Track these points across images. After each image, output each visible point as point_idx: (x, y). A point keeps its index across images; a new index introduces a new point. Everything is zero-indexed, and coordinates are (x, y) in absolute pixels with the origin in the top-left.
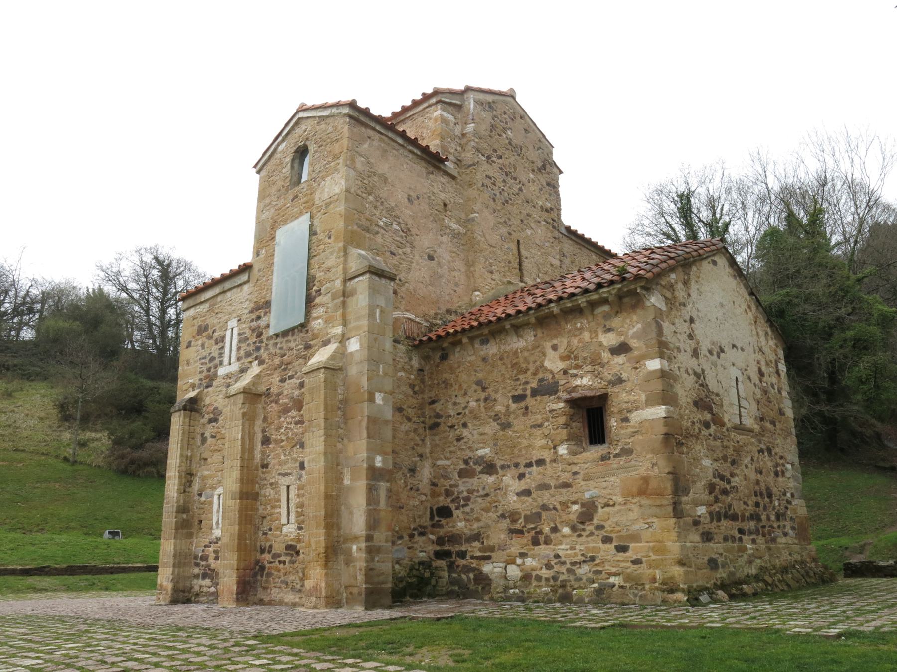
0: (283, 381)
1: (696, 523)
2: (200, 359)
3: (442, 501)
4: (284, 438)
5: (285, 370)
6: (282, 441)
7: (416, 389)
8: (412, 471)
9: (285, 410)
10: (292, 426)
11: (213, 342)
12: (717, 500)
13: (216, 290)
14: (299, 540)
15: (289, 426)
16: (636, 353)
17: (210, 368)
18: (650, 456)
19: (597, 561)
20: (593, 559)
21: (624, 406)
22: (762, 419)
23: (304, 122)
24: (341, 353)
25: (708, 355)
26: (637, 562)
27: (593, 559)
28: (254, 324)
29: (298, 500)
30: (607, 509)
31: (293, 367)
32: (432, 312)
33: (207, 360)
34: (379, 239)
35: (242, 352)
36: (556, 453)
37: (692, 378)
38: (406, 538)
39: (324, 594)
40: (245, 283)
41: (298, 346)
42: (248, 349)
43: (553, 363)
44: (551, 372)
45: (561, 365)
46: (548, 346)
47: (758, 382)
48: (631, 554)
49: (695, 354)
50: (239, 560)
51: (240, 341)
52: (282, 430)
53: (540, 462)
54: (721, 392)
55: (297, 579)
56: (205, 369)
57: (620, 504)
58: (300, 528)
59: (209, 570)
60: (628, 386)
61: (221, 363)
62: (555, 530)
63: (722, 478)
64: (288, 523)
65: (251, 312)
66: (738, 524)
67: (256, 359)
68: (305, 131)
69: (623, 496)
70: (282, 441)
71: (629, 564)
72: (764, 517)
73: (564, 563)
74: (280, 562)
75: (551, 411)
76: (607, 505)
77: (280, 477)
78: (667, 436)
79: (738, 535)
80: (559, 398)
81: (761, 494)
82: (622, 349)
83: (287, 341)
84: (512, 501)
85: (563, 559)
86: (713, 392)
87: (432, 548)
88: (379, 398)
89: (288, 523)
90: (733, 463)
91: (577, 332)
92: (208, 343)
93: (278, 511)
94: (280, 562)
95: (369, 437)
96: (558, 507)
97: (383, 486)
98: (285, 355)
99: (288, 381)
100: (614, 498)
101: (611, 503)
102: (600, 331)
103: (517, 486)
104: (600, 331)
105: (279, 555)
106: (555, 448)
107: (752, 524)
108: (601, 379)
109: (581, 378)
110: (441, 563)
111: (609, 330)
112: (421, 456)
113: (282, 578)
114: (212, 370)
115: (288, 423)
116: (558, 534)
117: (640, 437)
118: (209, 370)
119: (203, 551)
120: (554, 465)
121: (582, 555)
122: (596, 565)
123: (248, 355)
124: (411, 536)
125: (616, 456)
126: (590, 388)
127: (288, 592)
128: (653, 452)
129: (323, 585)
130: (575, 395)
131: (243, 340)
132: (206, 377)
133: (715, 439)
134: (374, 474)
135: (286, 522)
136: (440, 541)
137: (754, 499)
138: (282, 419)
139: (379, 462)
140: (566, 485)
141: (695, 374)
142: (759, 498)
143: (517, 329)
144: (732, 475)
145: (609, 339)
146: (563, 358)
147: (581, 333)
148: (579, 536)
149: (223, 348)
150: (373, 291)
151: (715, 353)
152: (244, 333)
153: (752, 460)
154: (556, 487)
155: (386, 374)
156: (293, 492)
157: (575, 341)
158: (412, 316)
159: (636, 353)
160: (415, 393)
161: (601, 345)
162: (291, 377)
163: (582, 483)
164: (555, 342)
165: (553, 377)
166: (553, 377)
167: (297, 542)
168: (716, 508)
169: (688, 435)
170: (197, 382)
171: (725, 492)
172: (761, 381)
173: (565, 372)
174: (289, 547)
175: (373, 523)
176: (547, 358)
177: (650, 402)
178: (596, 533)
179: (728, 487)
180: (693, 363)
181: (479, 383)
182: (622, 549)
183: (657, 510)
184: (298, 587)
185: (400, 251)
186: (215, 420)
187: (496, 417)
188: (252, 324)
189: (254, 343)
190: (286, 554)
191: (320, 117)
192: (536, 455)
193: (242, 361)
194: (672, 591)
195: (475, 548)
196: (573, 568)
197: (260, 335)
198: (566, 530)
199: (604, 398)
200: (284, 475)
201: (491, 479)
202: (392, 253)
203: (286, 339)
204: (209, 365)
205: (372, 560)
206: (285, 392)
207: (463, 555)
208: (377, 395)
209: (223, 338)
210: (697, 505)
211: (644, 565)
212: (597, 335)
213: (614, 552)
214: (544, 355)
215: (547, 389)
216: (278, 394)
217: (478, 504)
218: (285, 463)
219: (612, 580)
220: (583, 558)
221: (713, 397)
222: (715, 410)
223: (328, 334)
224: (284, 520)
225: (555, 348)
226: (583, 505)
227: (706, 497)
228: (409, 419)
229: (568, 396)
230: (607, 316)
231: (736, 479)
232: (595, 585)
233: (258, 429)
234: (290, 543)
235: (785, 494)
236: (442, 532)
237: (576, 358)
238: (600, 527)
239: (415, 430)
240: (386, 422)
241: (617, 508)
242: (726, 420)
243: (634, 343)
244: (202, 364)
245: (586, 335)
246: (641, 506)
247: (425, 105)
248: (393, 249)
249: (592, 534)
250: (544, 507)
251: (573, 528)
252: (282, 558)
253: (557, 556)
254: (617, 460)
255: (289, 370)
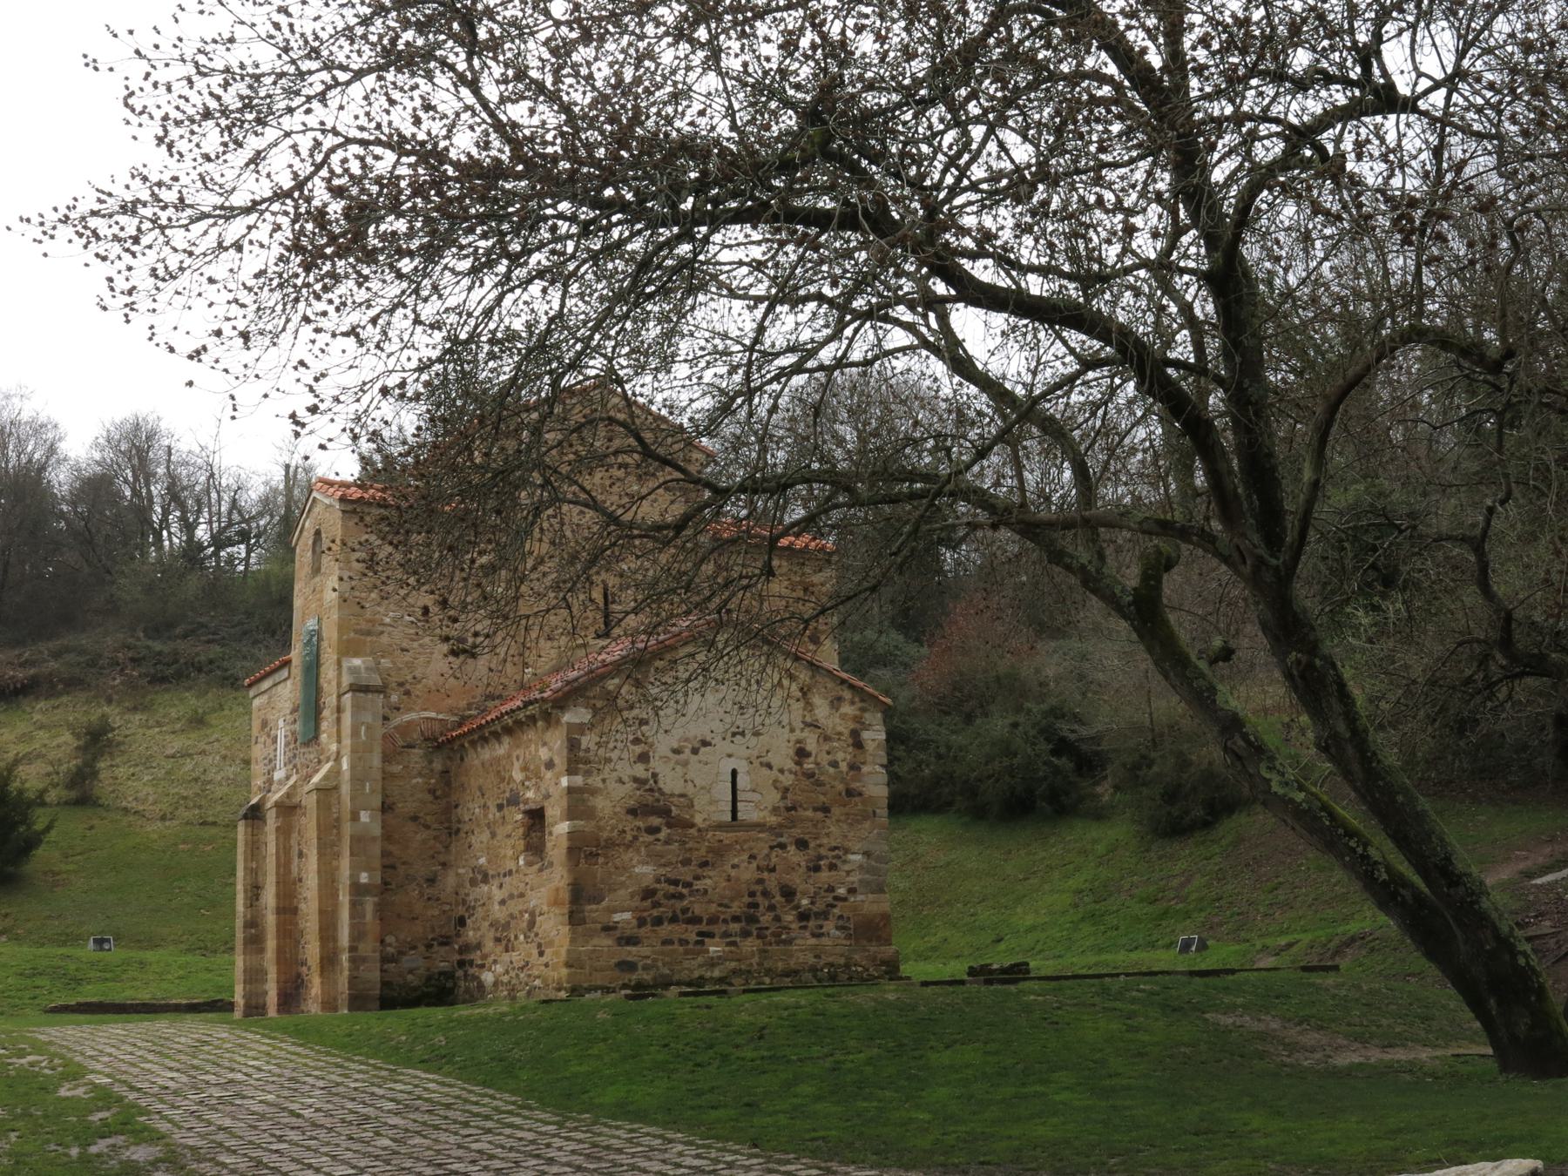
1: (608, 929)
3: (461, 911)
7: (439, 793)
8: (431, 881)
12: (656, 905)
22: (788, 809)
24: (336, 772)
25: (671, 755)
32: (463, 704)
34: (385, 639)
37: (630, 786)
38: (422, 948)
47: (790, 765)
49: (644, 758)
50: (279, 972)
53: (510, 872)
54: (690, 790)
62: (516, 937)
63: (675, 883)
66: (697, 928)
72: (766, 919)
78: (570, 850)
79: (693, 937)
81: (765, 894)
84: (498, 912)
86: (672, 795)
87: (457, 957)
88: (365, 817)
90: (704, 864)
95: (352, 854)
97: (370, 903)
103: (498, 895)
107: (735, 927)
110: (460, 973)
112: (444, 865)
124: (429, 946)
131: (287, 744)
133: (667, 843)
134: (357, 890)
136: (461, 951)
137: (747, 899)
139: (364, 878)
140: (522, 895)
141: (636, 780)
142: (759, 899)
143: (497, 736)
144: (697, 878)
145: (544, 754)
150: (357, 708)
151: (687, 751)
153: (753, 857)
155: (373, 791)
158: (433, 715)
160: (436, 798)
168: (655, 913)
169: (610, 844)
171: (681, 897)
172: (798, 763)
175: (357, 935)
177: (562, 820)
179: (685, 891)
180: (640, 770)
181: (480, 789)
185: (415, 644)
187: (488, 826)
192: (510, 865)
195: (476, 956)
199: (542, 809)
201: (485, 888)
202: (403, 650)
205: (357, 968)
207: (471, 963)
208: (362, 813)
209: (275, 741)
210: (615, 912)
215: (514, 800)
217: (480, 912)
221: (675, 800)
222: (675, 811)
227: (636, 902)
228: (427, 827)
231: (708, 881)
233: (293, 842)
235: (831, 889)
236: (461, 941)
239: (435, 838)
240: (374, 839)
242: (698, 819)
243: (557, 760)
245: (533, 747)
248: (404, 645)
250: (512, 916)
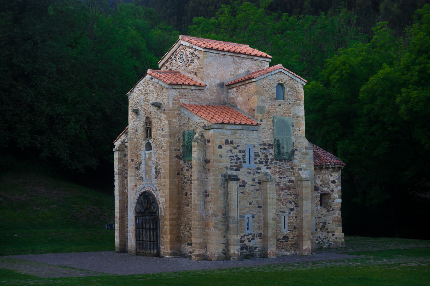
0: (281, 178)
2: (230, 157)
4: (282, 199)
5: (281, 174)
6: (282, 200)
9: (283, 189)
10: (286, 195)
11: (237, 151)
13: (239, 127)
14: (289, 234)
15: (284, 195)
16: (337, 184)
17: (238, 162)
18: (338, 211)
19: (328, 238)
20: (327, 237)
21: (334, 198)
23: (282, 73)
26: (336, 238)
27: (327, 237)
28: (263, 151)
29: (289, 221)
30: (329, 225)
31: (286, 174)
33: (235, 158)
35: (258, 161)
36: (317, 208)
39: (310, 250)
40: (255, 131)
41: (288, 167)
42: (261, 160)
43: (319, 182)
44: (318, 185)
45: (320, 183)
46: (317, 176)
48: (335, 236)
51: (255, 155)
52: (281, 196)
55: (288, 246)
56: (234, 162)
57: (331, 223)
58: (289, 230)
59: (245, 246)
60: (335, 192)
61: (245, 162)
64: (284, 228)
65: (260, 145)
67: (265, 166)
68: (284, 79)
69: (332, 221)
70: (282, 200)
71: (334, 239)
73: (321, 239)
74: (280, 242)
75: (317, 196)
76: (329, 223)
77: (281, 213)
80: (319, 192)
82: (334, 182)
83: (282, 164)
85: (321, 238)
89: (284, 228)
91: (324, 174)
92: (234, 150)
93: (281, 224)
94: (280, 242)
96: (317, 223)
98: (281, 168)
99: (283, 179)
100: (330, 222)
101: (329, 223)
102: (330, 176)
104: (330, 175)
105: (280, 239)
106: (317, 207)
108: (329, 189)
109: (325, 188)
111: (331, 176)
113: (282, 247)
114: (238, 164)
115: (284, 194)
116: (317, 231)
117: (336, 206)
118: (236, 163)
119: (241, 239)
120: (317, 212)
121: (325, 237)
122: (328, 239)
123: (261, 163)
125: (331, 211)
126: (326, 191)
127: (284, 251)
128: (339, 210)
129: (310, 248)
130: (323, 192)
132: (235, 166)
135: (283, 228)
138: (281, 192)
140: (320, 218)
145: (331, 179)
146: (321, 181)
147: (325, 175)
148: (322, 231)
149: (245, 155)
152: (258, 153)
154: (317, 218)
156: (287, 219)
157: (324, 177)
159: (337, 184)
161: (329, 179)
162: (284, 178)
163: (323, 217)
164: (319, 175)
165: (318, 186)
166: (318, 186)
167: (289, 235)
170: (229, 167)
173: (321, 185)
174: (284, 237)
176: (317, 180)
177: (339, 198)
178: (326, 231)
182: (333, 235)
183: (339, 225)
184: (289, 249)
186: (244, 186)
188: (261, 150)
189: (265, 159)
190: (283, 239)
191: (291, 77)
193: (258, 165)
194: (343, 245)
196: (323, 240)
197: (266, 156)
198: (319, 230)
200: (283, 212)
203: (281, 162)
204: (236, 161)
206: (282, 183)
211: (338, 239)
212: (329, 176)
213: (332, 235)
214: (316, 179)
216: (279, 183)
218: (284, 208)
219: (331, 243)
220: (325, 237)
223: (301, 166)
224: (283, 227)
225: (319, 177)
226: (323, 223)
229: (321, 193)
230: (331, 172)
232: (328, 244)
234: (285, 235)
237: (323, 182)
238: (327, 229)
241: (330, 224)
243: (337, 181)
244: (231, 159)
245: (327, 176)
246: (336, 224)
247: (264, 59)
249: (325, 231)
251: (321, 229)
252: (282, 240)
253: (319, 237)
254: (331, 212)
255: (284, 175)
